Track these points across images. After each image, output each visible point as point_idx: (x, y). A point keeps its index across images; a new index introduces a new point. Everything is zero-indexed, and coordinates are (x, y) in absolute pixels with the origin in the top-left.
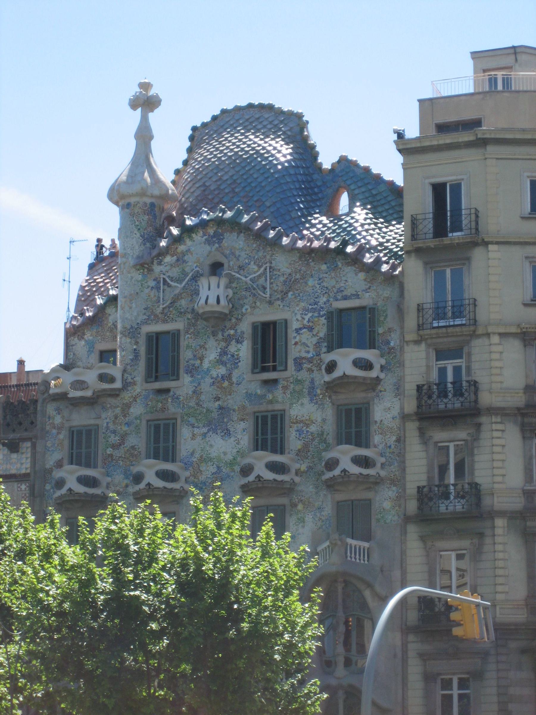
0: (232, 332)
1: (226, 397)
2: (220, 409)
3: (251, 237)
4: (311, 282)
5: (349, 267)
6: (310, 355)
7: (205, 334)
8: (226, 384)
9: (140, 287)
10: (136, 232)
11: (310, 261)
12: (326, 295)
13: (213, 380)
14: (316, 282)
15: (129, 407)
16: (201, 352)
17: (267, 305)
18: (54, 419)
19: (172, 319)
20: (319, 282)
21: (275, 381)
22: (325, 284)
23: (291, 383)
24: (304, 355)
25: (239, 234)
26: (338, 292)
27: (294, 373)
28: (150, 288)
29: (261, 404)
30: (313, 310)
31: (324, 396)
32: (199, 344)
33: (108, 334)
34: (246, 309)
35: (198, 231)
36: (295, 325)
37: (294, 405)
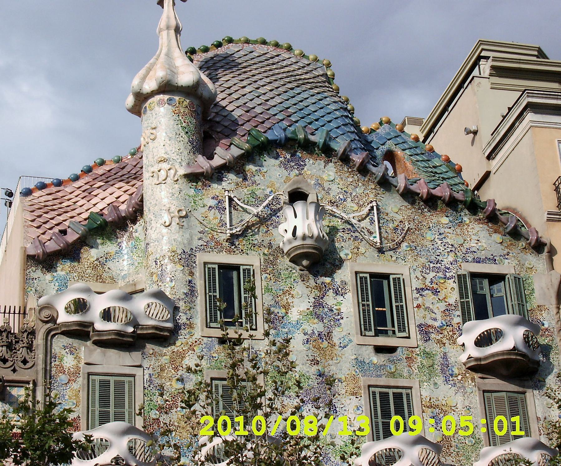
0: (328, 280)
1: (327, 361)
2: (320, 375)
3: (346, 170)
4: (429, 236)
5: (481, 226)
6: (437, 324)
7: (291, 277)
8: (325, 344)
9: (193, 204)
10: (183, 134)
11: (426, 210)
12: (452, 254)
13: (307, 337)
14: (437, 237)
15: (183, 358)
16: (285, 298)
17: (376, 254)
18: (61, 360)
19: (242, 251)
20: (440, 237)
21: (391, 350)
22: (448, 240)
23: (418, 355)
24: (430, 322)
25: (327, 163)
26: (467, 253)
27: (420, 343)
28: (207, 208)
29: (380, 376)
30: (438, 270)
31: (464, 376)
32: (281, 288)
33: (89, 271)
34: (347, 255)
35: (271, 149)
36: (416, 284)
37: (425, 384)
